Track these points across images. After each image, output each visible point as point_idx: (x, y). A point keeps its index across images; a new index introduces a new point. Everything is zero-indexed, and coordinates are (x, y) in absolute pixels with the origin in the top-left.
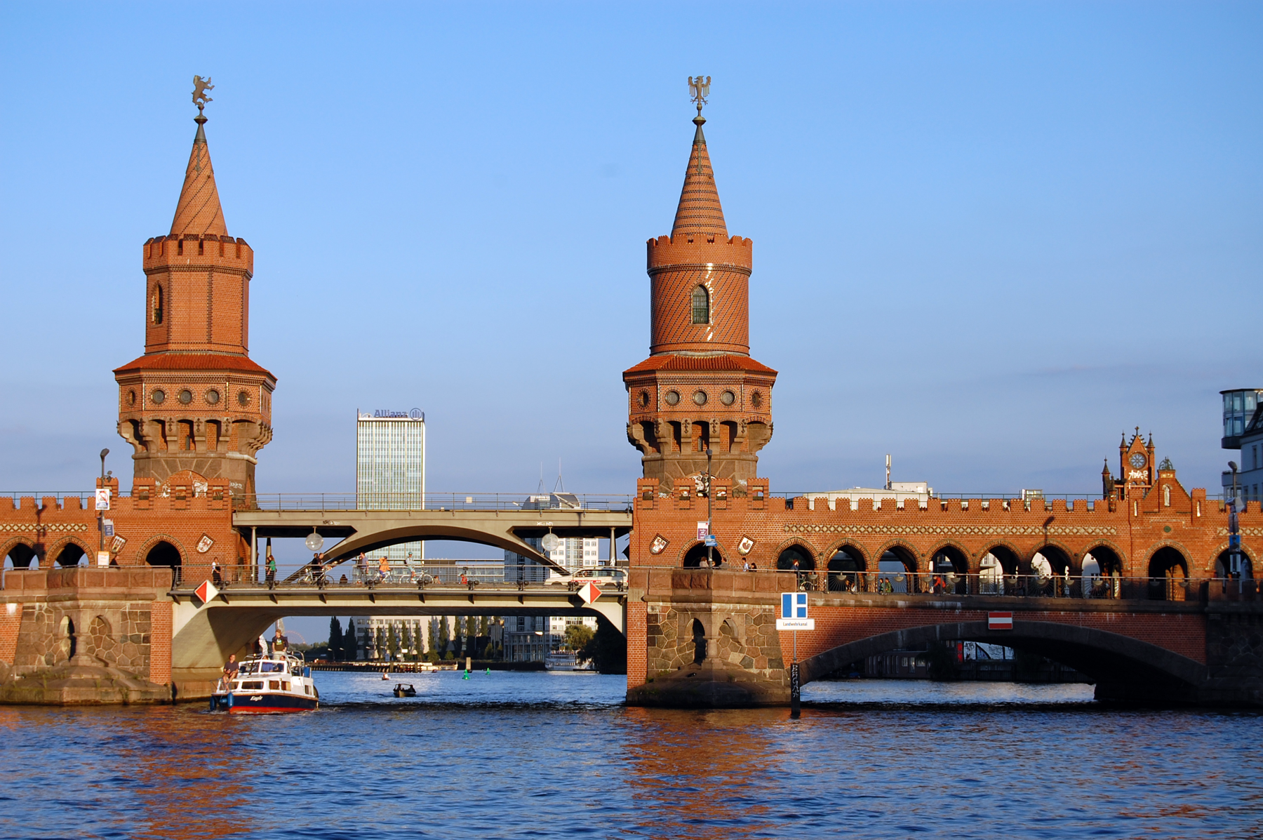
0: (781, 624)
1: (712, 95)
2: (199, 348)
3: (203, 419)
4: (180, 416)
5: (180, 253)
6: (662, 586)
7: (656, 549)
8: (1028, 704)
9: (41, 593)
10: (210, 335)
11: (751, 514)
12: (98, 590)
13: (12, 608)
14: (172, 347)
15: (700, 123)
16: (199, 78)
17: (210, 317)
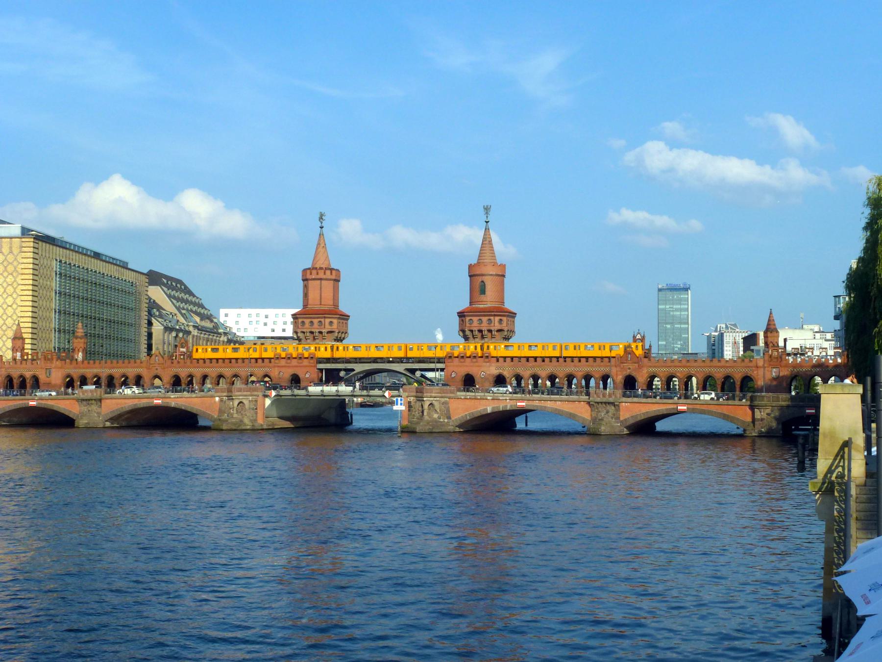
0: (395, 408)
1: (491, 213)
2: (317, 307)
3: (317, 331)
4: (309, 330)
5: (311, 274)
6: (412, 392)
7: (453, 376)
8: (520, 434)
9: (225, 394)
10: (321, 302)
11: (485, 364)
12: (240, 393)
13: (217, 399)
14: (309, 306)
15: (487, 222)
16: (321, 212)
17: (321, 295)
